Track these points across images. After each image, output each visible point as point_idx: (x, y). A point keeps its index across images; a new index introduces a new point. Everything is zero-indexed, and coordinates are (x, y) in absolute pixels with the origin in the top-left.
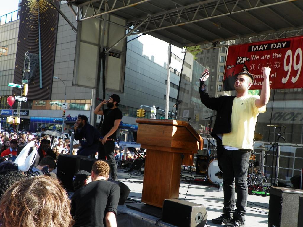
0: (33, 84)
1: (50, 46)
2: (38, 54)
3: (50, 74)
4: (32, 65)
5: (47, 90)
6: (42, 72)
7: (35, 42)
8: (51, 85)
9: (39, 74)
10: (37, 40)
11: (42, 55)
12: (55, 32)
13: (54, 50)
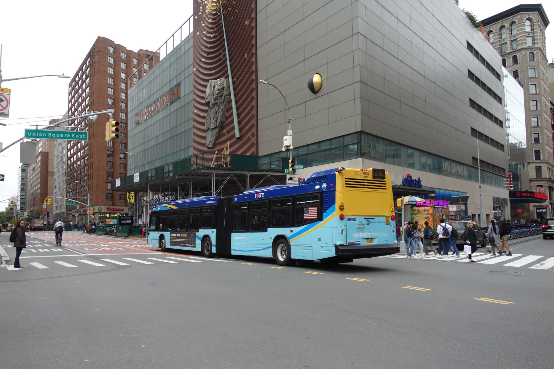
0: (224, 135)
1: (246, 55)
2: (227, 77)
3: (253, 107)
4: (218, 101)
5: (249, 139)
6: (238, 109)
7: (221, 59)
8: (255, 128)
9: (232, 114)
10: (223, 54)
11: (233, 78)
12: (253, 25)
13: (253, 59)
